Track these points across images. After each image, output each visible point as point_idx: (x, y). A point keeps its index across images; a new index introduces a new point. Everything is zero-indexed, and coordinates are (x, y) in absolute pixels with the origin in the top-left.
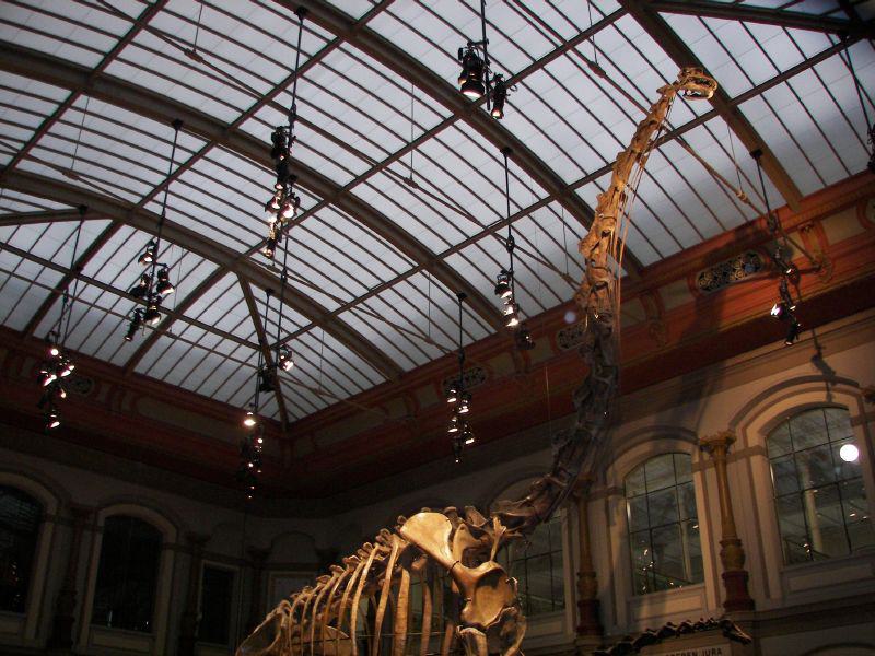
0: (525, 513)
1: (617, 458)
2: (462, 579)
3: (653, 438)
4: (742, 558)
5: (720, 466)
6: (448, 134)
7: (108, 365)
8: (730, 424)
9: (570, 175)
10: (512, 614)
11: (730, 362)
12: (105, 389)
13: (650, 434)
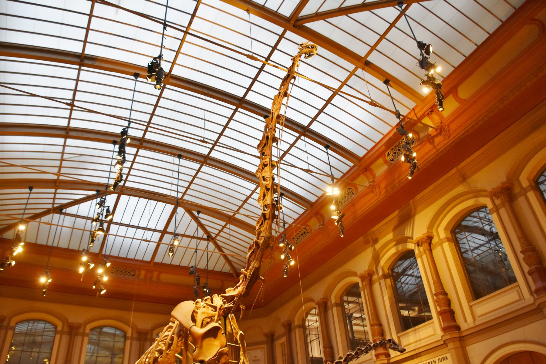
1: (381, 259)
2: (195, 334)
3: (395, 245)
4: (448, 302)
5: (427, 252)
6: (237, 116)
7: (142, 261)
8: (428, 228)
10: (225, 352)
11: (418, 197)
12: (143, 273)
13: (394, 243)
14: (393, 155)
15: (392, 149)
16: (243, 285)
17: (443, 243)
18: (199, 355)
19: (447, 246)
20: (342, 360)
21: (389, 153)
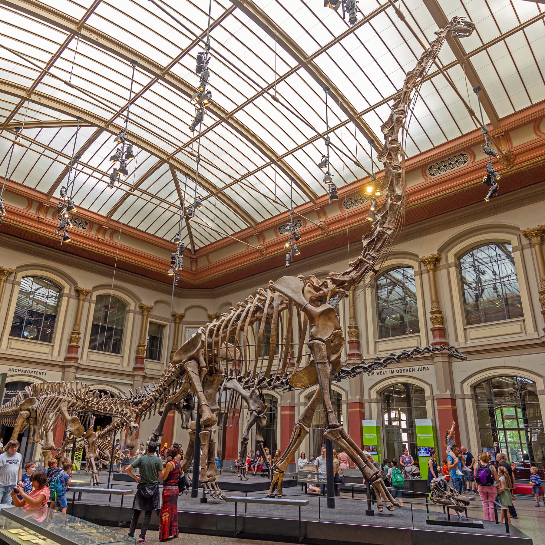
0: (346, 278)
4: (442, 321)
5: (431, 273)
9: (359, 106)
14: (433, 169)
15: (437, 164)
16: (357, 273)
17: (450, 267)
18: (317, 332)
19: (453, 270)
20: (395, 357)
21: (431, 166)
